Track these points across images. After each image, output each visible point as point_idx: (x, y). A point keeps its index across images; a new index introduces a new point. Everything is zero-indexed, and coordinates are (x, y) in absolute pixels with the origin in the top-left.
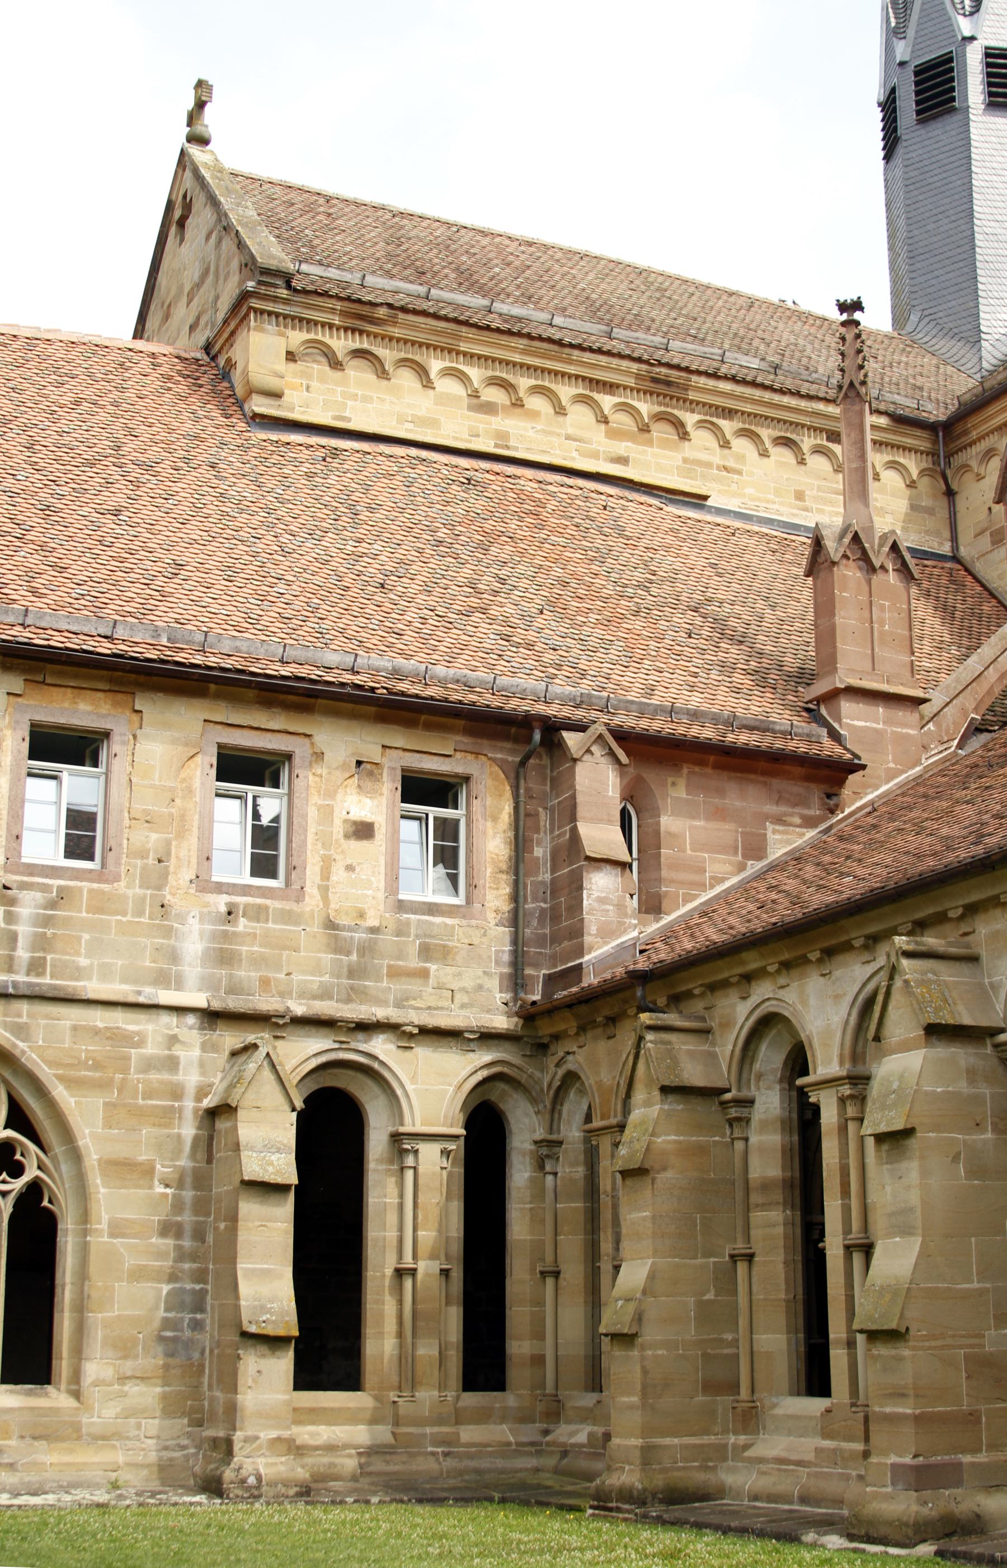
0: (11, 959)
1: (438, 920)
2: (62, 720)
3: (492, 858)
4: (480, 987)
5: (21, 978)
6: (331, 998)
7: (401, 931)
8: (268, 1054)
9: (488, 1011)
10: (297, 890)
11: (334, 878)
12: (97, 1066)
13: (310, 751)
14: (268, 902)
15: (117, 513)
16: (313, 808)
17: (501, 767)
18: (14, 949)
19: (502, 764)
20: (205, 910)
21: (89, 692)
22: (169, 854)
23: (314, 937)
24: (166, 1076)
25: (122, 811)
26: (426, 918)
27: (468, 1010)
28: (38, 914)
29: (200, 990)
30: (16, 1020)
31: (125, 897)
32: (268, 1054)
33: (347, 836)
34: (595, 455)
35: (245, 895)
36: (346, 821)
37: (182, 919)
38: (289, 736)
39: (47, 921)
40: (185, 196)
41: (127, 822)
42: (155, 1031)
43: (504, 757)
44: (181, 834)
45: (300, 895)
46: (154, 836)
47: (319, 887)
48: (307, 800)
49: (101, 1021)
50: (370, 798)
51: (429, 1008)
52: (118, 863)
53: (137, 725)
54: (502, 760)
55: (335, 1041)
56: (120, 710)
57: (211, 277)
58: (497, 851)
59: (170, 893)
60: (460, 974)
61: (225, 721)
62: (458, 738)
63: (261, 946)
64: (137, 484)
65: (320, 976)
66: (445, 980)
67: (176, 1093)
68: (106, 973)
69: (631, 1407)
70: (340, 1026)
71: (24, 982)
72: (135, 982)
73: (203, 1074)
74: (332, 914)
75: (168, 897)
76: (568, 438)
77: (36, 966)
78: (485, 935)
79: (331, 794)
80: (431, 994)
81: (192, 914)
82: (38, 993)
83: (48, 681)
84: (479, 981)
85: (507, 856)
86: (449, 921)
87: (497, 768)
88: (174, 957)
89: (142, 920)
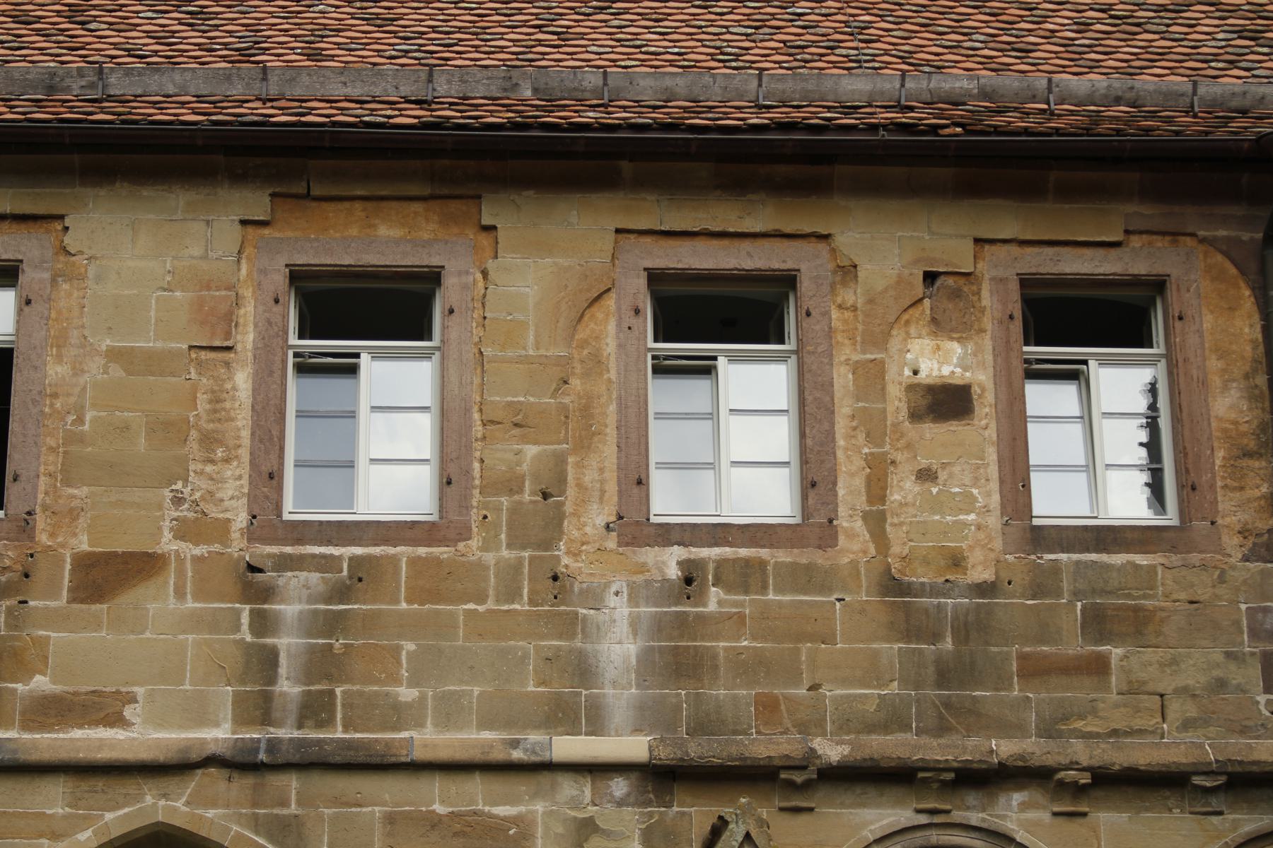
0: (266, 699)
1: (1118, 559)
2: (346, 259)
3: (1225, 431)
4: (1221, 685)
5: (286, 733)
6: (906, 727)
7: (1044, 583)
8: (748, 836)
9: (1244, 731)
10: (821, 525)
13: (831, 266)
14: (764, 553)
16: (843, 369)
17: (1226, 254)
18: (272, 679)
19: (1228, 249)
20: (639, 578)
21: (394, 204)
22: (562, 480)
23: (862, 612)
25: (468, 411)
26: (1093, 557)
27: (1200, 732)
28: (316, 612)
29: (637, 730)
30: (276, 811)
31: (481, 566)
32: (748, 836)
33: (915, 416)
35: (717, 545)
36: (911, 388)
37: (594, 598)
38: (787, 243)
39: (332, 624)
41: (478, 430)
42: (548, 814)
43: (1233, 234)
44: (585, 442)
46: (531, 450)
47: (866, 517)
48: (831, 356)
49: (442, 802)
50: (959, 340)
51: (1115, 733)
53: (489, 252)
54: (1228, 239)
55: (919, 811)
56: (456, 230)
58: (1233, 416)
59: (568, 553)
60: (1174, 662)
61: (658, 228)
62: (1131, 208)
63: (754, 638)
65: (879, 687)
66: (1143, 676)
68: (450, 713)
70: (924, 780)
71: (291, 740)
72: (508, 725)
74: (895, 566)
75: (565, 560)
78: (1222, 579)
79: (879, 339)
80: (1117, 706)
81: (614, 588)
82: (314, 758)
83: (316, 191)
84: (1217, 673)
85: (1256, 422)
86: (1141, 560)
87: (1220, 258)
89: (517, 607)
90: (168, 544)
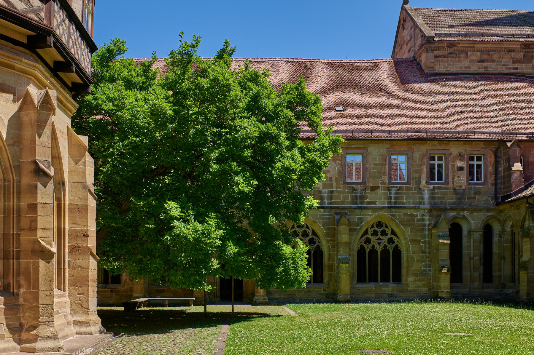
1: (478, 186)
11: (455, 179)
12: (408, 221)
15: (402, 103)
18: (391, 200)
24: (422, 223)
31: (412, 187)
33: (458, 170)
34: (509, 68)
36: (457, 167)
37: (424, 191)
39: (397, 194)
40: (404, 18)
45: (448, 184)
46: (417, 174)
52: (411, 181)
57: (413, 39)
60: (483, 197)
64: (405, 95)
67: (424, 225)
69: (524, 286)
73: (429, 221)
76: (503, 65)
77: (395, 203)
86: (480, 186)
88: (423, 198)
90: (380, 185)
